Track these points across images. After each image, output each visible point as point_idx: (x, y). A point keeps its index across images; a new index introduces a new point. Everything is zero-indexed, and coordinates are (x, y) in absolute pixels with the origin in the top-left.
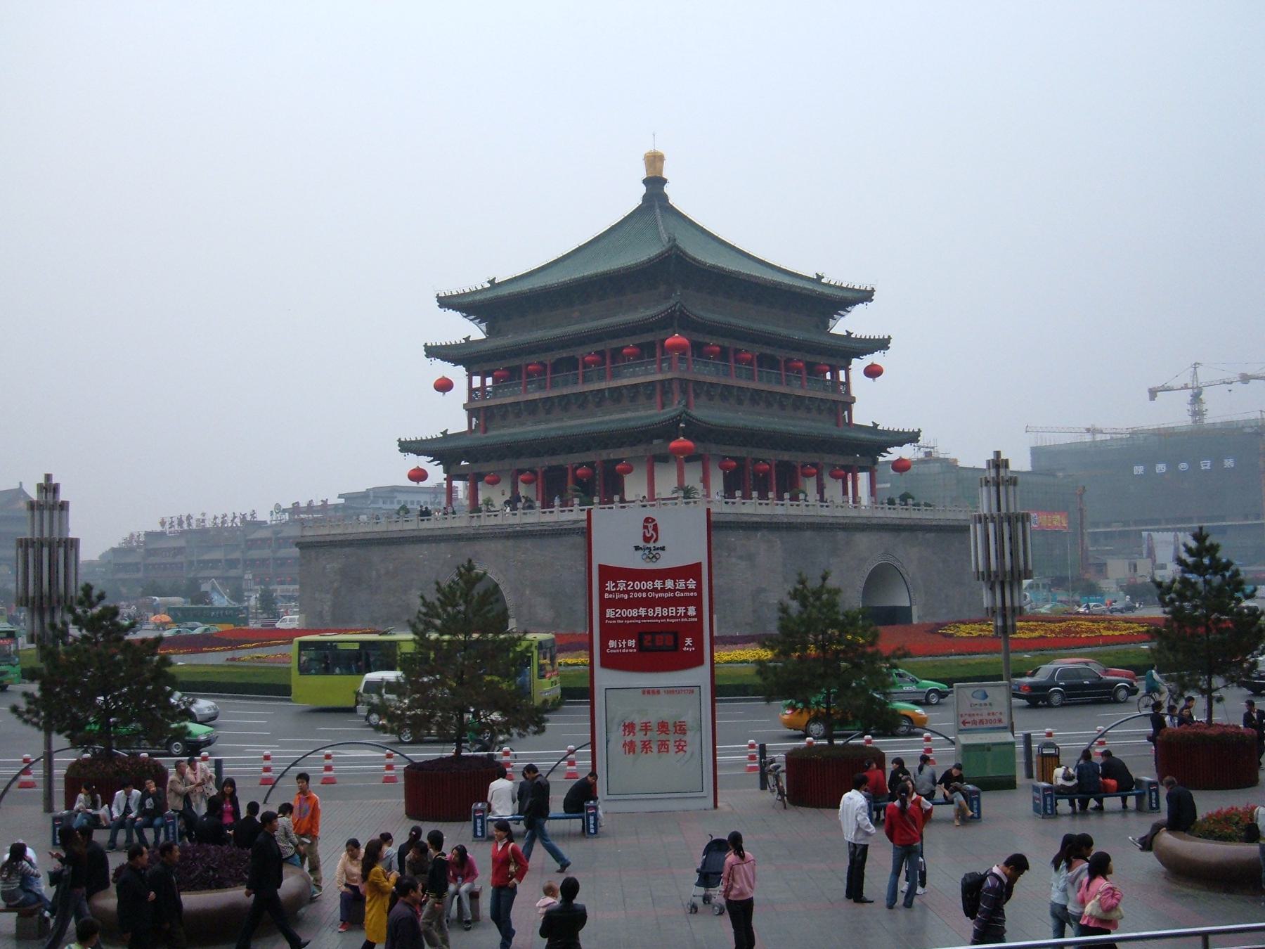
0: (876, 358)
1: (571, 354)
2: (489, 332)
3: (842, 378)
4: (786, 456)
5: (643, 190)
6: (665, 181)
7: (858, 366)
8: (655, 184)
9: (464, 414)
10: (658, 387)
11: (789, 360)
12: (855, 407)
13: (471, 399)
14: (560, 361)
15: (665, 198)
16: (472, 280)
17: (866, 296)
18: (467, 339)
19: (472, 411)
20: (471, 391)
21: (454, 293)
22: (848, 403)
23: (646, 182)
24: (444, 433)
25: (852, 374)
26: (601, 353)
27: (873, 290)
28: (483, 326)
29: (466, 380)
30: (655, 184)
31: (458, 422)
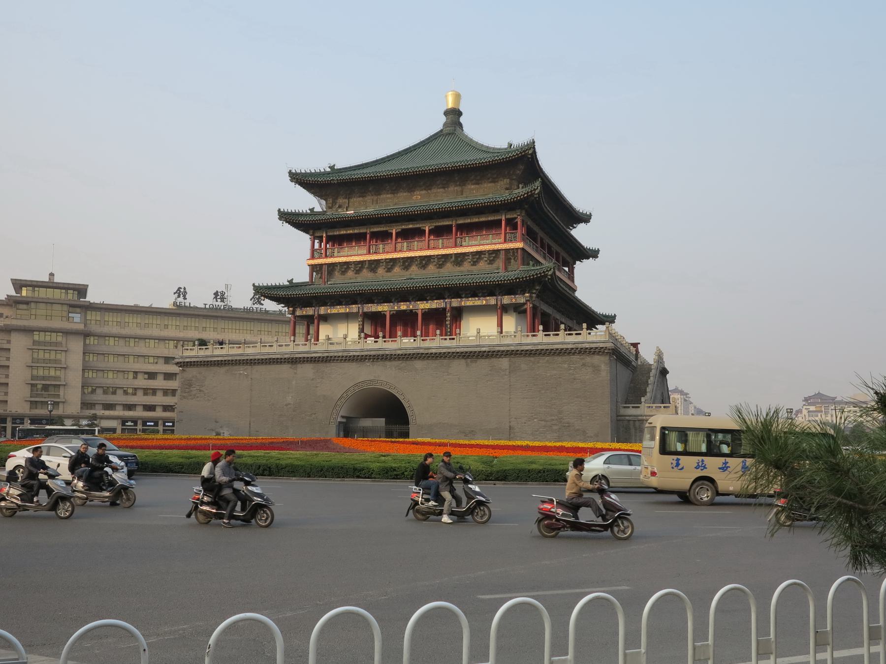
1: (418, 226)
6: (460, 114)
8: (454, 115)
9: (307, 270)
10: (502, 255)
14: (403, 230)
15: (460, 125)
16: (317, 163)
18: (312, 210)
19: (314, 268)
20: (313, 250)
21: (303, 171)
23: (447, 113)
24: (291, 281)
27: (590, 215)
29: (309, 243)
30: (454, 115)
31: (302, 275)
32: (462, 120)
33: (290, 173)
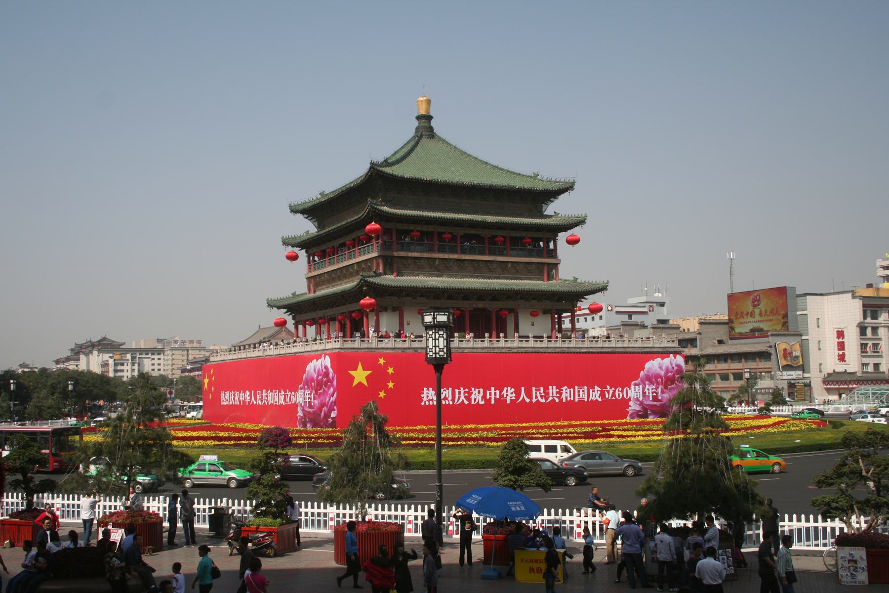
0: (576, 231)
2: (320, 227)
3: (551, 246)
4: (480, 305)
5: (416, 123)
7: (562, 237)
9: (305, 282)
11: (494, 237)
12: (560, 267)
13: (310, 270)
17: (568, 188)
18: (307, 233)
22: (556, 266)
25: (558, 243)
26: (354, 240)
28: (316, 224)
30: (426, 119)
32: (433, 123)
33: (290, 207)
